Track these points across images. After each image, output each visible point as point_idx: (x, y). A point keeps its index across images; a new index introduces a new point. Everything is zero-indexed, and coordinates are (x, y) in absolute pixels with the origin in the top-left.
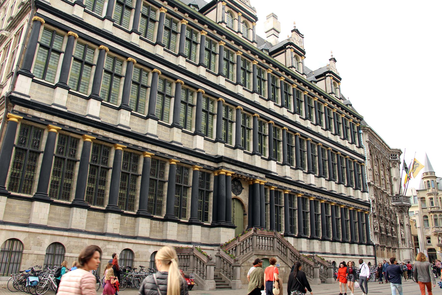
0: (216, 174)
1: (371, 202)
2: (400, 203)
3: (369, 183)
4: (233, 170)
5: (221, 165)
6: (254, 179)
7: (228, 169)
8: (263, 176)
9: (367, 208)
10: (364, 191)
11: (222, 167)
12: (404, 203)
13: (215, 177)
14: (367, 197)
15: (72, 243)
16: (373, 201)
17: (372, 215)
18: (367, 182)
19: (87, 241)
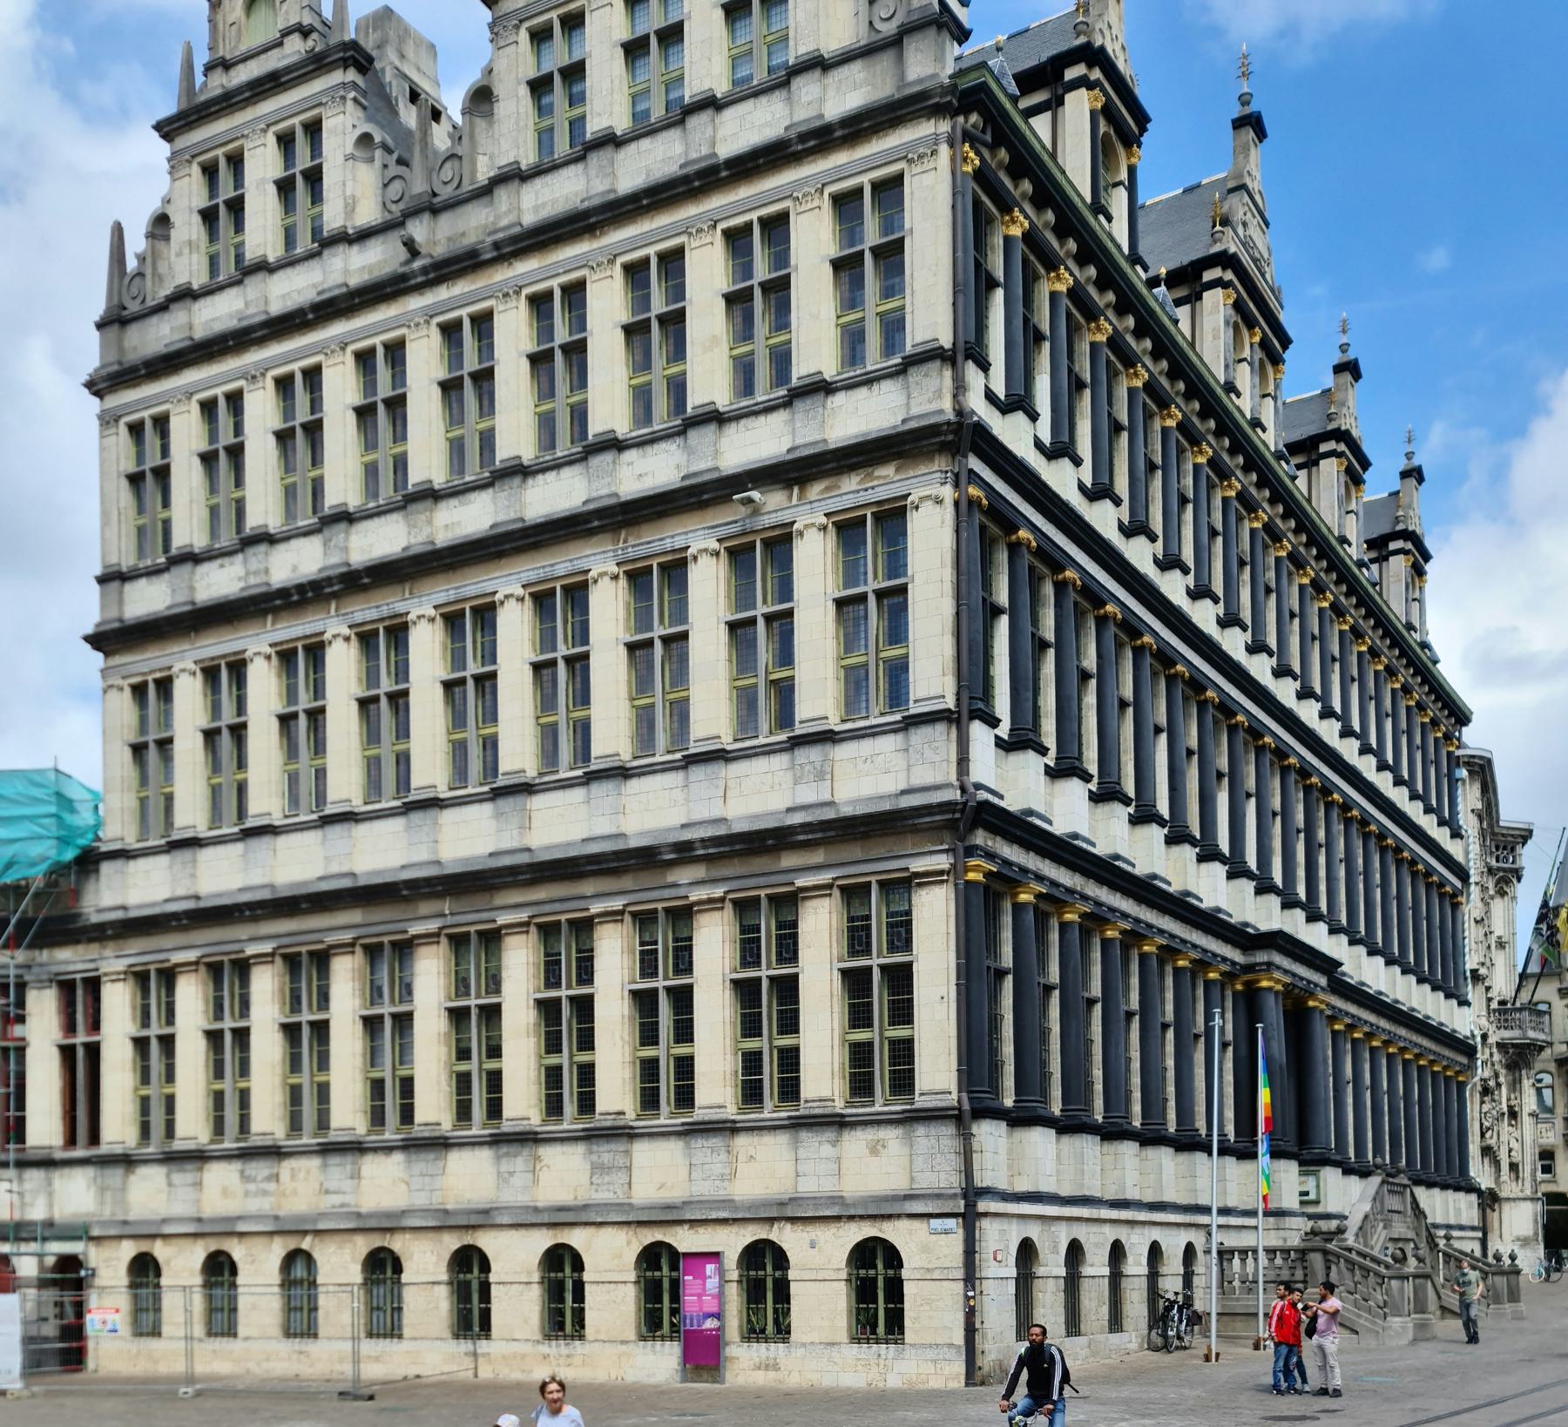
0: (1239, 987)
1: (1479, 1039)
2: (1516, 1033)
3: (1474, 972)
4: (1286, 972)
5: (1261, 957)
6: (1312, 995)
7: (1278, 968)
8: (1323, 981)
9: (1464, 1060)
10: (1464, 1003)
11: (1269, 964)
12: (1531, 1034)
13: (1235, 994)
14: (1465, 1021)
15: (1093, 1239)
16: (1484, 1037)
17: (1479, 1088)
18: (1468, 967)
19: (1107, 1229)
